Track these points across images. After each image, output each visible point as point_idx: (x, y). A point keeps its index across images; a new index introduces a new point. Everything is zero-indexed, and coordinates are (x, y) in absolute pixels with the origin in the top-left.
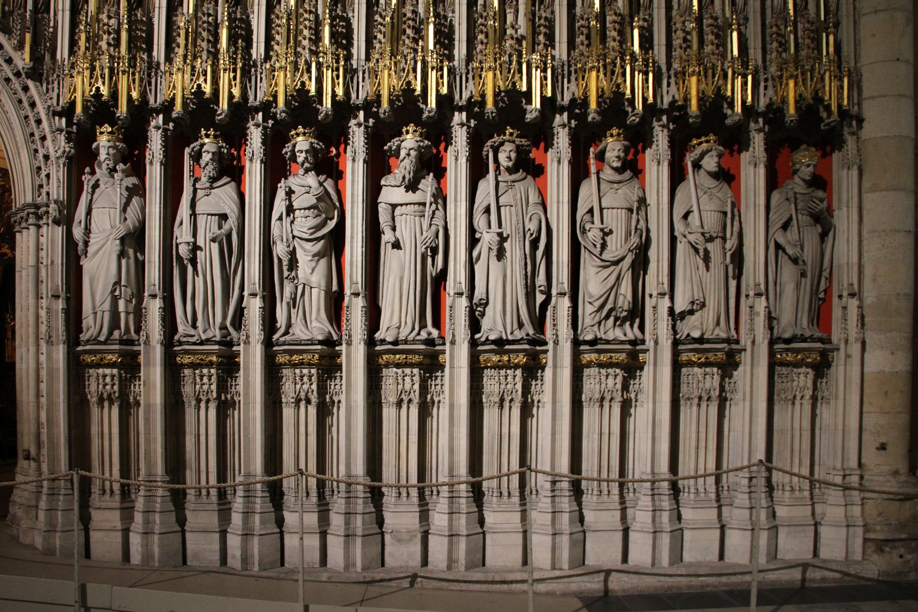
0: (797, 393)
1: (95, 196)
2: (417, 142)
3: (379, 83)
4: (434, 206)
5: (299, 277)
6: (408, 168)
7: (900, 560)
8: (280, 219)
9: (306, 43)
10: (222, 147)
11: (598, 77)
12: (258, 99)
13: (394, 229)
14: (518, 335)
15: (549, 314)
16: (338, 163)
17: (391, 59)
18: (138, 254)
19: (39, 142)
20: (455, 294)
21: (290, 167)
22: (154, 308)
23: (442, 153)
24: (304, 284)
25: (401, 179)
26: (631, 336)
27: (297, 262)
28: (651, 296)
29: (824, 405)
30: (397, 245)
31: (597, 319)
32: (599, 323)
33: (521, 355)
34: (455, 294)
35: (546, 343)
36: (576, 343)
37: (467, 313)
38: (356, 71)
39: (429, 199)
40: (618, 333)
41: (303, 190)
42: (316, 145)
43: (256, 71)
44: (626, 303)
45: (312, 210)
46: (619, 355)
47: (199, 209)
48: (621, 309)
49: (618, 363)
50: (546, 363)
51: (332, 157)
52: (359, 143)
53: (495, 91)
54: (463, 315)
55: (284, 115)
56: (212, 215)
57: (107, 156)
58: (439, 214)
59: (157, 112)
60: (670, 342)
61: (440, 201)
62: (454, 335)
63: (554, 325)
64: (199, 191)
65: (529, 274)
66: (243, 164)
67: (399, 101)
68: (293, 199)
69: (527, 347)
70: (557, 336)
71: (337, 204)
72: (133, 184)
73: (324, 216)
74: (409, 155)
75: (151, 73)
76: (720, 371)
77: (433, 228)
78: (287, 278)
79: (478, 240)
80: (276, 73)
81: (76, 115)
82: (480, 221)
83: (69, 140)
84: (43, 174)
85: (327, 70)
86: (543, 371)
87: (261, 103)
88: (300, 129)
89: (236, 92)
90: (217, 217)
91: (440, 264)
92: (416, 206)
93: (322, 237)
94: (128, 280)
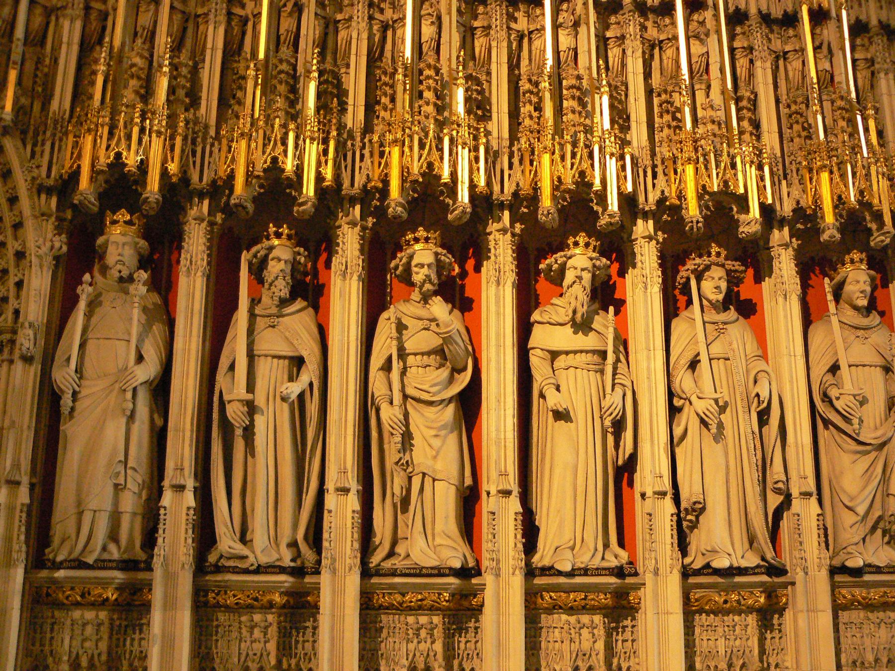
1: (94, 320)
2: (591, 259)
5: (415, 462)
8: (387, 367)
11: (831, 180)
12: (356, 185)
13: (558, 389)
14: (751, 560)
16: (463, 287)
17: (553, 139)
18: (156, 416)
19: (9, 232)
20: (655, 493)
21: (391, 289)
24: (424, 474)
30: (561, 415)
32: (864, 539)
41: (421, 324)
42: (443, 258)
45: (433, 357)
50: (786, 603)
52: (504, 257)
53: (697, 192)
54: (668, 528)
55: (399, 209)
56: (279, 357)
58: (622, 367)
59: (201, 195)
61: (622, 349)
64: (258, 319)
66: (321, 282)
68: (404, 338)
69: (765, 578)
75: (196, 138)
78: (397, 463)
79: (679, 410)
80: (387, 149)
81: (78, 192)
82: (684, 381)
84: (12, 280)
86: (781, 615)
88: (421, 233)
90: (287, 362)
91: (629, 449)
93: (450, 400)
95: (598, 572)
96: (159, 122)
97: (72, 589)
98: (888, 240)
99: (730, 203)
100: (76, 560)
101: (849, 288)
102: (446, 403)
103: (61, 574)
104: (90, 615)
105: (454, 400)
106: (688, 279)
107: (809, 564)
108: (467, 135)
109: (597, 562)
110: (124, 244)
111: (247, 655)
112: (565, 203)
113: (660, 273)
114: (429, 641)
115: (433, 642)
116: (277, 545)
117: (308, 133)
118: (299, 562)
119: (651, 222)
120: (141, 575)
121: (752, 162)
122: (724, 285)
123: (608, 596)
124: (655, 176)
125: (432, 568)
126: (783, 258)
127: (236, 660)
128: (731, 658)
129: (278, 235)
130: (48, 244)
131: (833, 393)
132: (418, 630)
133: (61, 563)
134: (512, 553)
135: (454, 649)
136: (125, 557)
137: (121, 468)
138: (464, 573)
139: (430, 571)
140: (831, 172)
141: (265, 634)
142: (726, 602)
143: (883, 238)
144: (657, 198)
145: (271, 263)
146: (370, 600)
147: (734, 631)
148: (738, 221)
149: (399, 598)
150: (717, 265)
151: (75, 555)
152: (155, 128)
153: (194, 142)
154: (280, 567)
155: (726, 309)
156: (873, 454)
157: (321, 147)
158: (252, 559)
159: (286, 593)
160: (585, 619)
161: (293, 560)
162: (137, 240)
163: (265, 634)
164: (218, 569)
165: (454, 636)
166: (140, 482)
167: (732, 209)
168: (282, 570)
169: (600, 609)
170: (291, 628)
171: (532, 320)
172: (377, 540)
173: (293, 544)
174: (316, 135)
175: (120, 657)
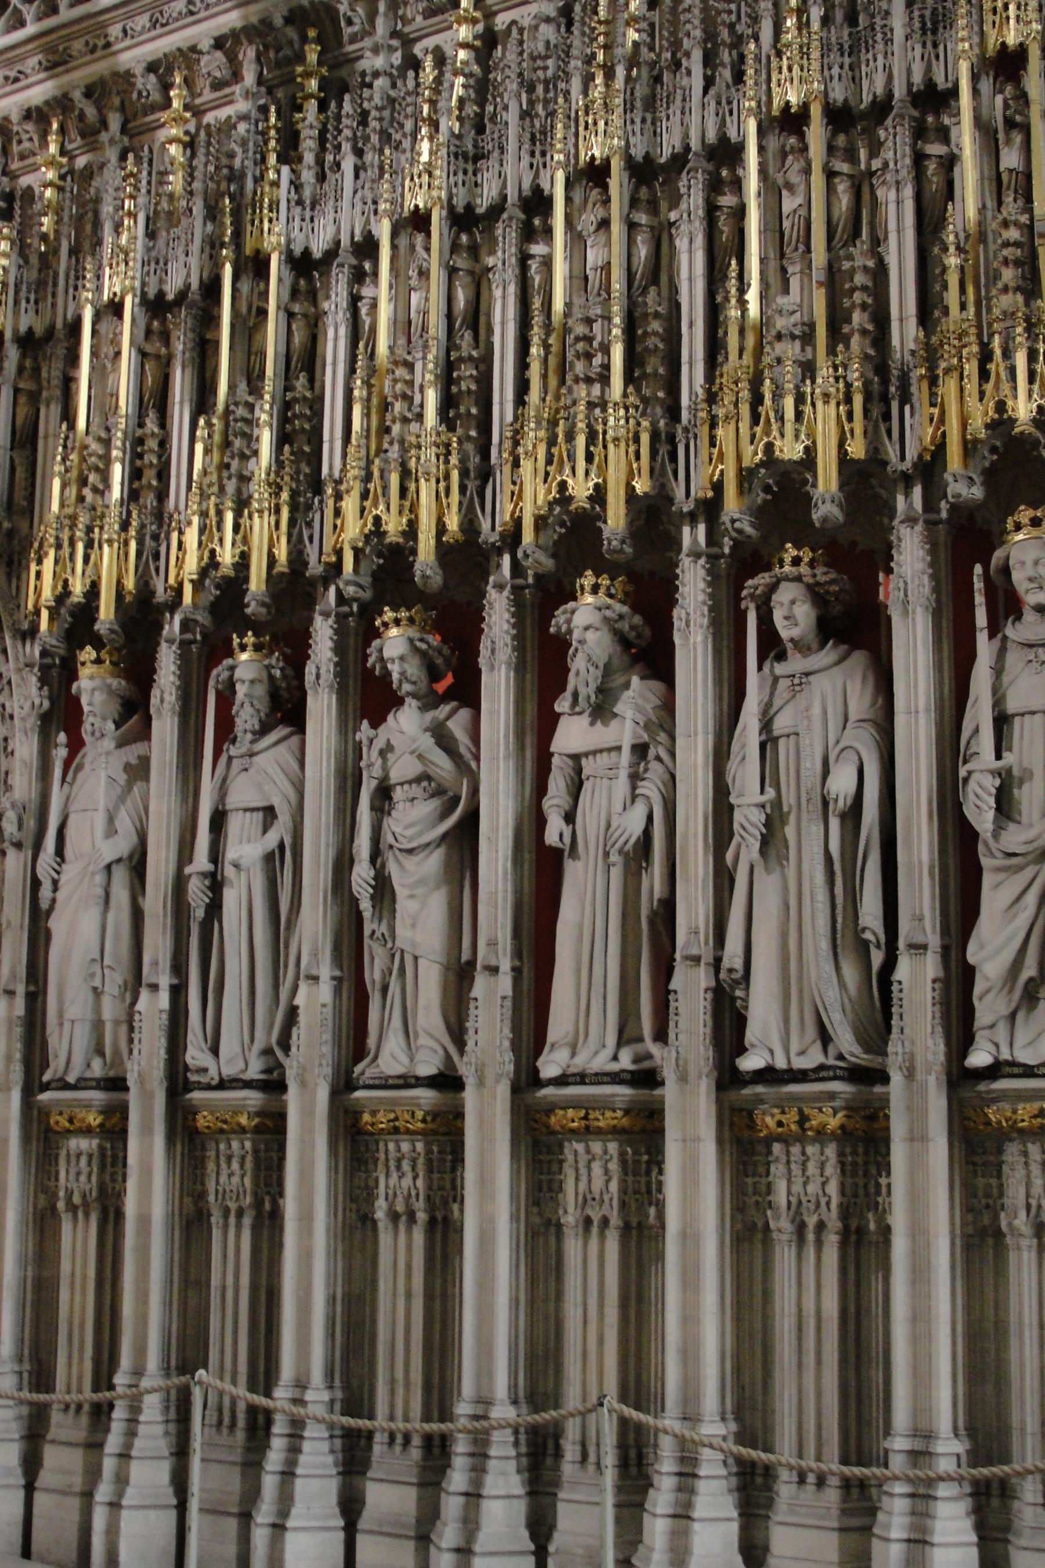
2: (600, 609)
14: (813, 1059)
42: (418, 644)
45: (425, 784)
47: (233, 801)
52: (501, 627)
64: (235, 761)
68: (389, 763)
88: (389, 615)
90: (261, 814)
97: (61, 1113)
100: (61, 1079)
102: (432, 847)
108: (434, 459)
109: (601, 1063)
110: (93, 690)
111: (225, 1191)
112: (563, 531)
115: (415, 1178)
118: (275, 1074)
125: (399, 1077)
128: (798, 1212)
129: (243, 648)
132: (399, 1161)
133: (48, 1083)
136: (112, 1074)
137: (97, 968)
145: (238, 687)
147: (804, 1170)
150: (786, 579)
151: (59, 1075)
152: (106, 536)
155: (822, 645)
158: (213, 1072)
159: (258, 1114)
160: (597, 1147)
161: (267, 1071)
162: (109, 681)
166: (120, 981)
168: (248, 1084)
171: (557, 708)
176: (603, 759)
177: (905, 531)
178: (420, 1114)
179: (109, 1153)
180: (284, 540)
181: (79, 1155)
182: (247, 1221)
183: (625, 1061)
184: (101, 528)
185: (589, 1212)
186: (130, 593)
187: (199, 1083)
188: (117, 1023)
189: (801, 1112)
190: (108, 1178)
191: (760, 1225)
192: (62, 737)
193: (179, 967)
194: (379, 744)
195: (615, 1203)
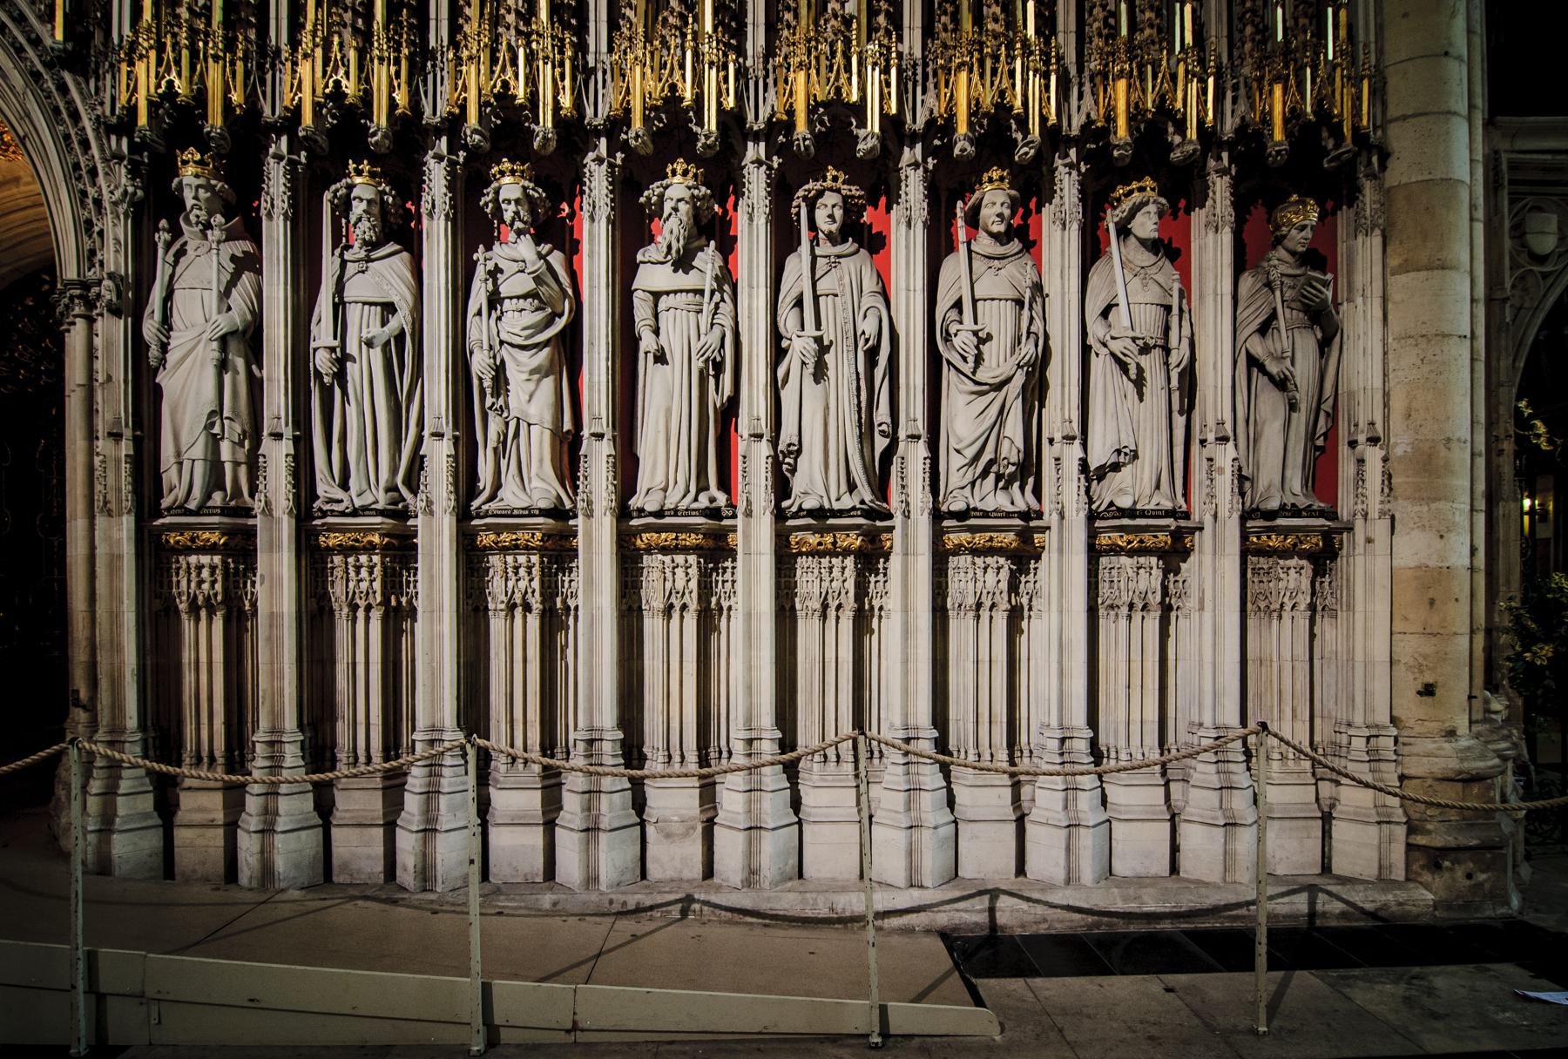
0: (1286, 600)
1: (179, 270)
2: (689, 188)
3: (628, 88)
4: (717, 297)
6: (675, 232)
7: (1468, 882)
8: (479, 313)
9: (511, 18)
10: (383, 193)
13: (657, 332)
14: (847, 502)
15: (894, 469)
17: (645, 48)
18: (254, 367)
20: (751, 436)
21: (499, 233)
22: (277, 455)
23: (731, 212)
24: (518, 419)
25: (665, 250)
26: (1021, 506)
27: (507, 383)
28: (1051, 441)
29: (1326, 619)
30: (661, 358)
31: (969, 477)
32: (973, 484)
33: (853, 534)
34: (751, 436)
35: (890, 516)
36: (937, 516)
37: (769, 466)
38: (594, 70)
39: (708, 284)
40: (1000, 501)
41: (516, 267)
42: (531, 192)
43: (434, 66)
44: (1015, 451)
45: (530, 300)
46: (1003, 535)
47: (349, 294)
48: (1005, 462)
49: (1001, 547)
51: (564, 218)
55: (477, 137)
56: (371, 304)
57: (195, 202)
58: (726, 308)
60: (1083, 515)
61: (726, 287)
62: (749, 502)
63: (903, 487)
65: (863, 405)
67: (661, 120)
70: (908, 504)
71: (570, 292)
72: (244, 252)
73: (549, 310)
74: (676, 209)
76: (1161, 562)
77: (717, 330)
78: (490, 408)
79: (785, 351)
80: (464, 68)
83: (134, 173)
85: (545, 63)
87: (443, 120)
89: (401, 97)
90: (379, 308)
91: (727, 390)
92: (691, 295)
93: (546, 343)
94: (234, 409)
95: (688, 512)
96: (216, 44)
98: (1032, 151)
99: (849, 117)
100: (181, 507)
101: (984, 212)
103: (168, 520)
104: (205, 559)
105: (552, 343)
106: (799, 206)
107: (911, 508)
111: (354, 593)
113: (767, 202)
114: (527, 578)
115: (531, 580)
116: (377, 489)
117: (376, 52)
118: (400, 506)
119: (762, 145)
120: (251, 522)
121: (875, 64)
122: (838, 213)
123: (701, 536)
124: (765, 90)
126: (911, 180)
127: (344, 598)
128: (826, 599)
129: (359, 173)
130: (121, 190)
131: (953, 329)
132: (516, 569)
134: (605, 494)
135: (557, 587)
136: (233, 503)
138: (559, 513)
139: (521, 512)
140: (971, 71)
141: (371, 573)
142: (820, 544)
143: (1026, 149)
144: (767, 115)
145: (354, 203)
146: (474, 541)
147: (831, 573)
148: (857, 137)
149: (493, 537)
150: (831, 189)
153: (261, 67)
154: (376, 510)
155: (845, 241)
156: (992, 395)
157: (393, 69)
160: (680, 559)
162: (213, 182)
163: (371, 573)
164: (324, 514)
165: (556, 575)
167: (851, 124)
168: (381, 513)
169: (692, 548)
170: (401, 569)
171: (639, 257)
172: (481, 485)
173: (391, 488)
174: (386, 54)
175: (241, 597)
176: (682, 299)
177: (910, 172)
178: (538, 535)
179: (232, 566)
180: (404, 87)
181: (200, 568)
182: (376, 615)
183: (703, 501)
184: (206, 44)
185: (673, 600)
186: (240, 106)
187: (332, 511)
188: (236, 464)
189: (835, 537)
190: (231, 586)
191: (787, 607)
192: (163, 223)
193: (301, 418)
194: (491, 266)
195: (695, 595)
